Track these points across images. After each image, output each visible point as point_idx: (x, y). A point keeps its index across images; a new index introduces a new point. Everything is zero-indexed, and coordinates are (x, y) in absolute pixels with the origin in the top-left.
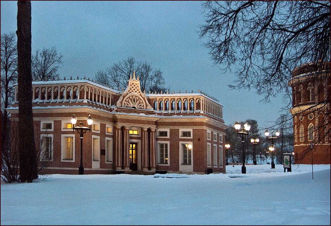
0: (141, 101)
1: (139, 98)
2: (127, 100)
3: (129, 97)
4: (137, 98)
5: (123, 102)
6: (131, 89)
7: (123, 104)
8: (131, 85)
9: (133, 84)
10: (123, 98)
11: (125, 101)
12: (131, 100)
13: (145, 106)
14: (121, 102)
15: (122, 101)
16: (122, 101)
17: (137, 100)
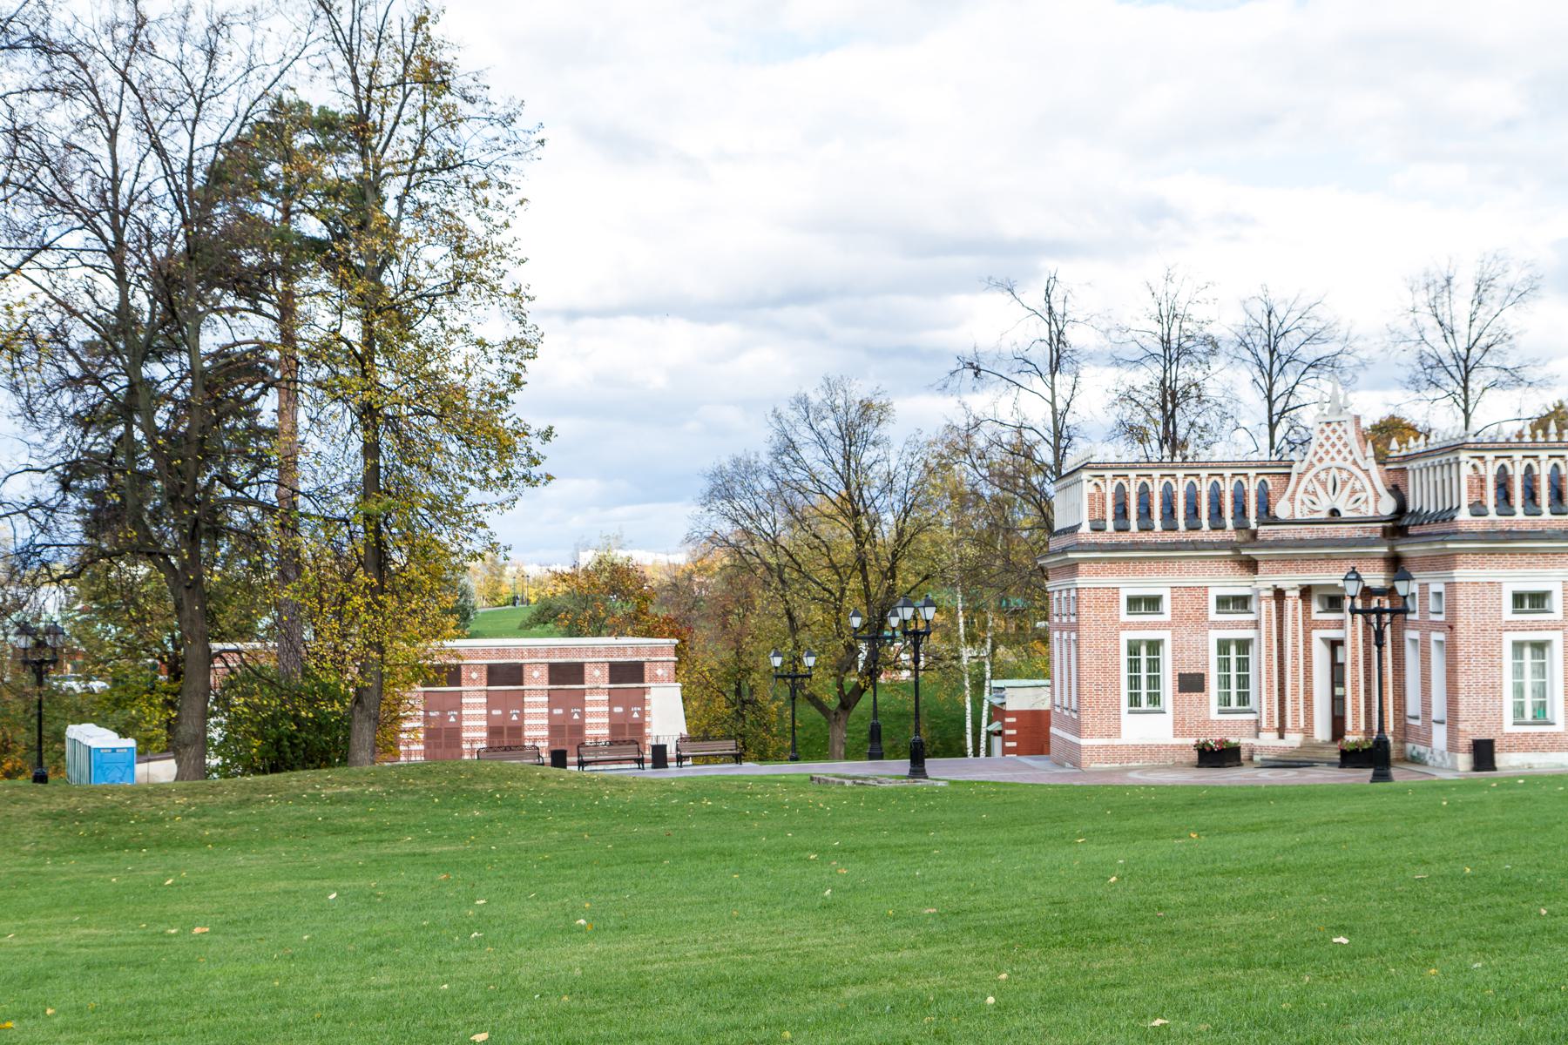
0: (1358, 486)
1: (1352, 474)
2: (1310, 489)
3: (1316, 476)
4: (1345, 475)
5: (1300, 495)
6: (1321, 445)
7: (1298, 504)
8: (1322, 431)
9: (1328, 424)
10: (1298, 483)
11: (1306, 491)
12: (1324, 484)
13: (1371, 500)
14: (1292, 499)
15: (1294, 492)
16: (1294, 492)
17: (1344, 483)
